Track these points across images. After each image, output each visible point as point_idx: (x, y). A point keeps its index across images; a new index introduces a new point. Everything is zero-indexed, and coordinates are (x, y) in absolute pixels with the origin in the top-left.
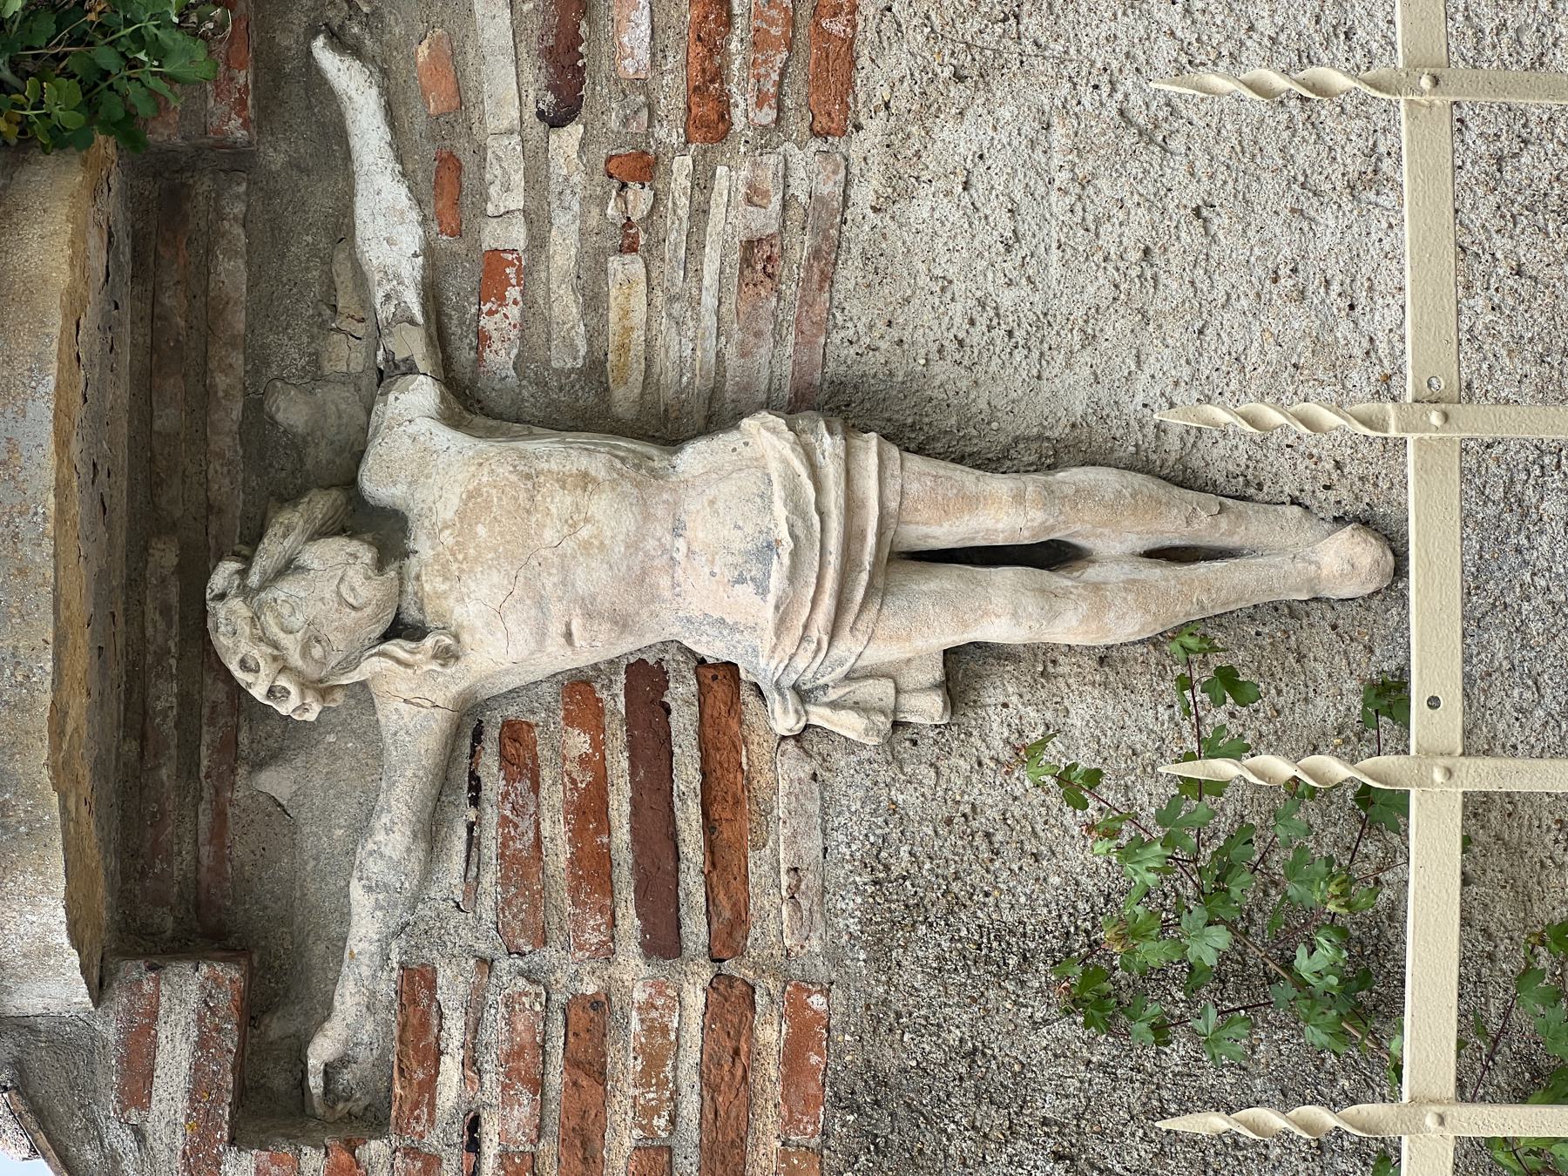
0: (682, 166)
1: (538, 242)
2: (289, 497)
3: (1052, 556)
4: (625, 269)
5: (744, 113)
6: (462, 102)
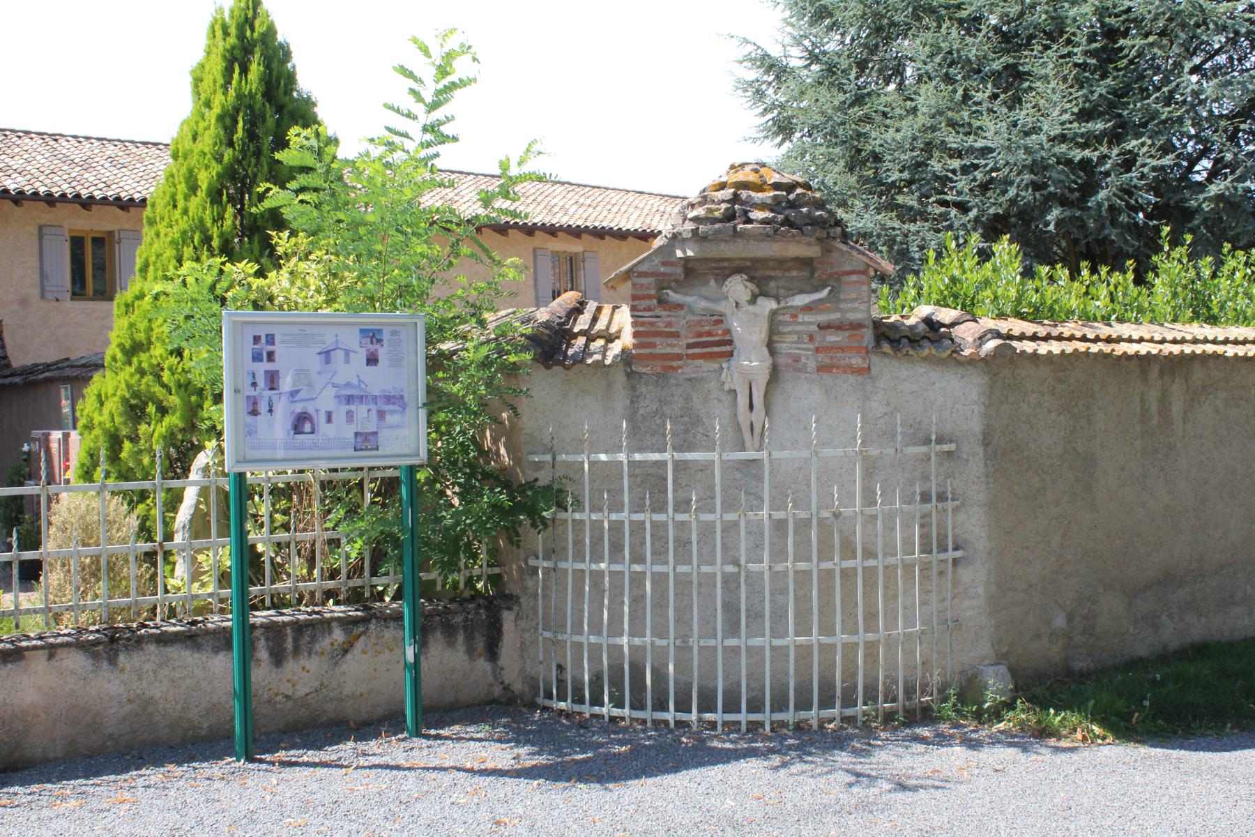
0: (811, 346)
1: (800, 324)
2: (758, 286)
3: (751, 407)
4: (795, 338)
5: (820, 356)
6: (820, 311)
